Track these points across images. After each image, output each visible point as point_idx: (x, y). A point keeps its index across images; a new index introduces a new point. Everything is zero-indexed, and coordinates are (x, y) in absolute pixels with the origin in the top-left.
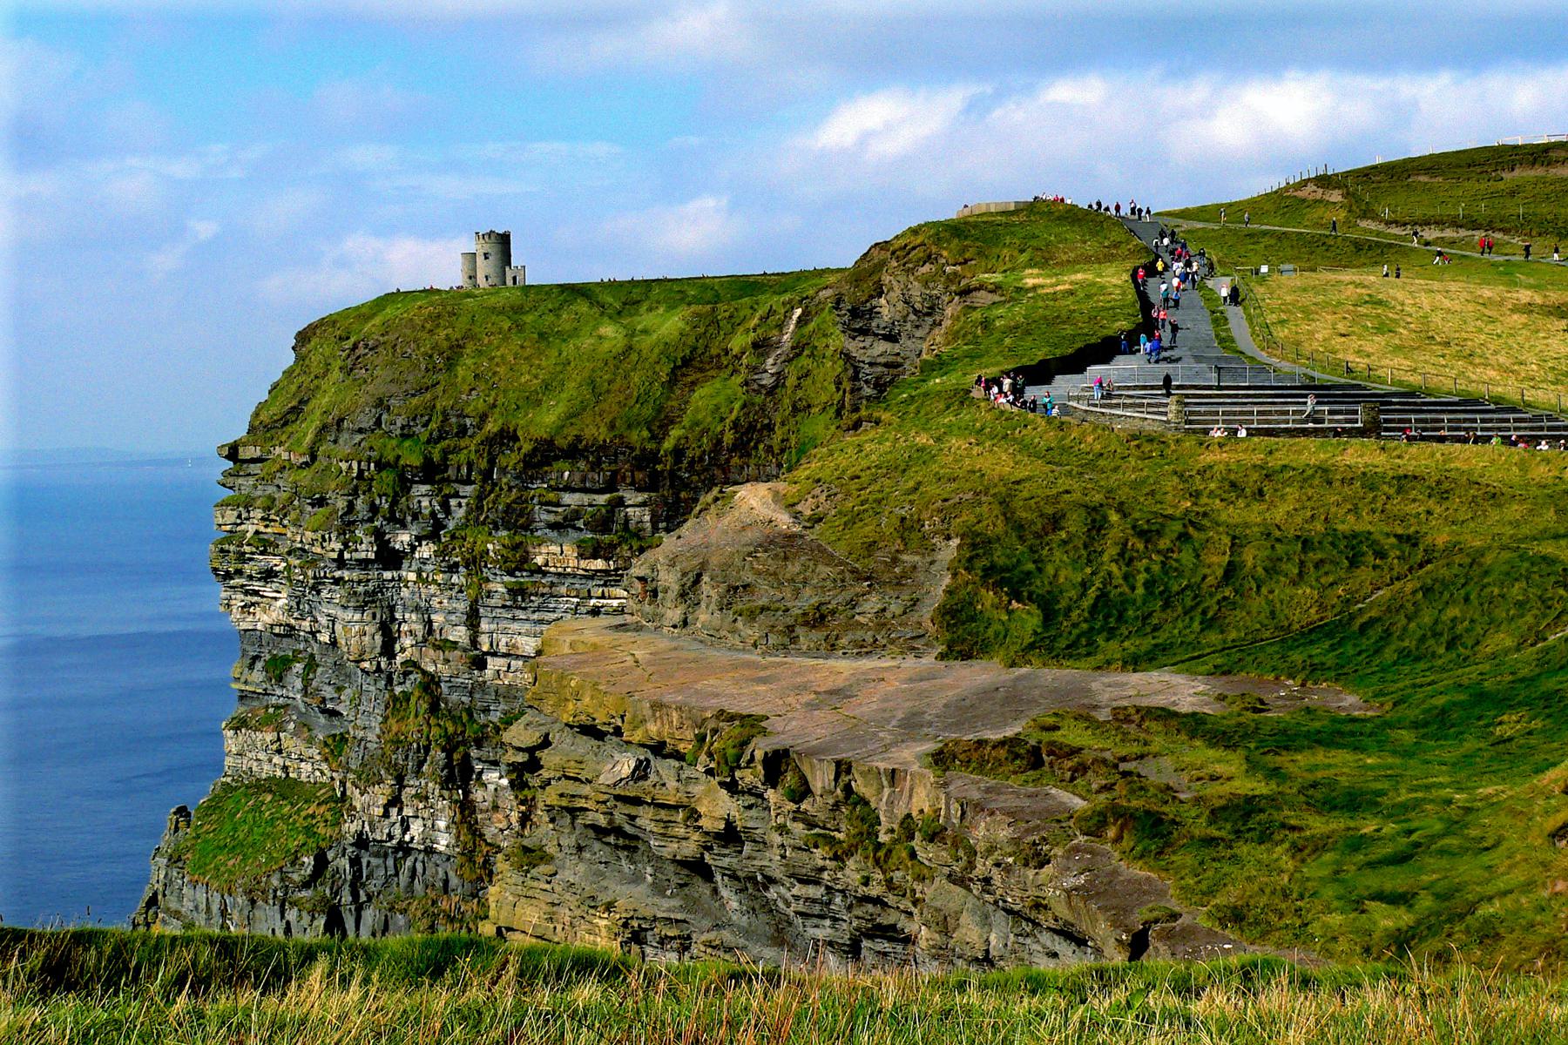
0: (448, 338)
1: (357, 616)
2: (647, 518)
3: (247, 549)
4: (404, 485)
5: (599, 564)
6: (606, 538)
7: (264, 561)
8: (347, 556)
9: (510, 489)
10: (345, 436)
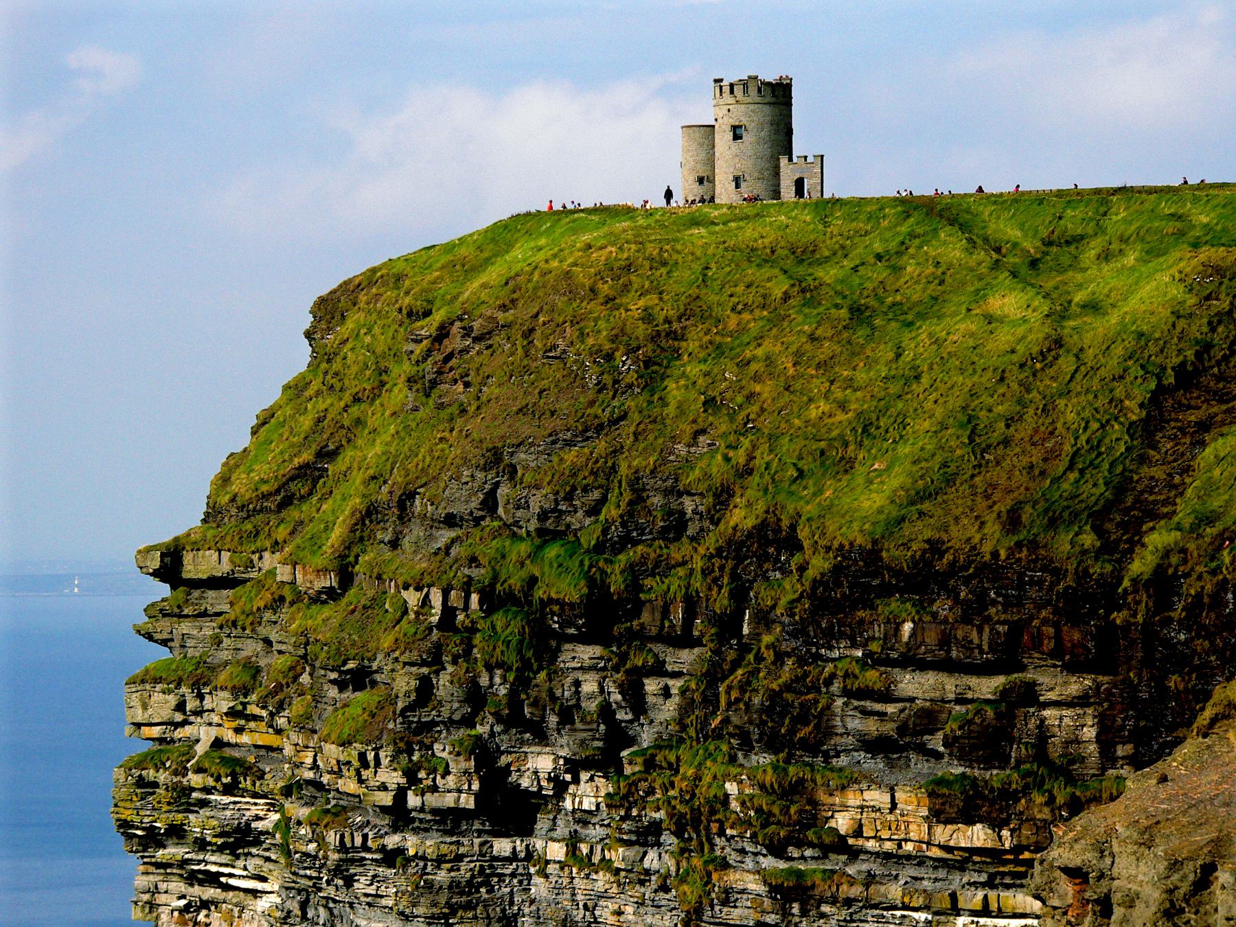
0: (648, 317)
2: (1089, 733)
3: (195, 780)
4: (542, 645)
5: (978, 835)
6: (995, 776)
7: (228, 809)
8: (413, 800)
9: (780, 658)
10: (415, 532)
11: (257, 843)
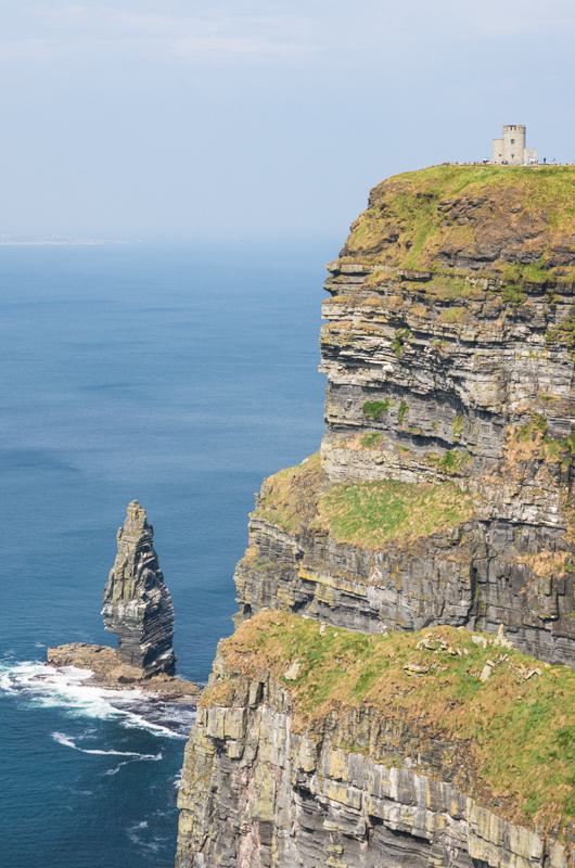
1: (486, 378)
11: (381, 350)
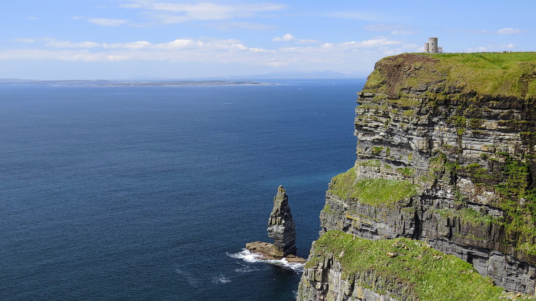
1: (422, 138)
